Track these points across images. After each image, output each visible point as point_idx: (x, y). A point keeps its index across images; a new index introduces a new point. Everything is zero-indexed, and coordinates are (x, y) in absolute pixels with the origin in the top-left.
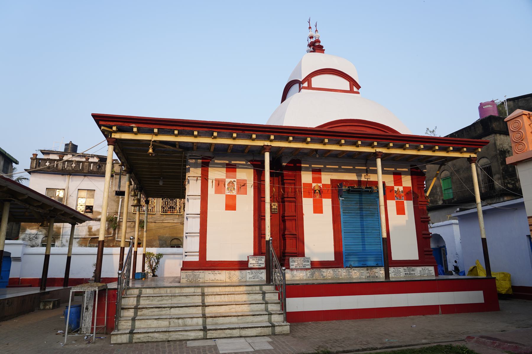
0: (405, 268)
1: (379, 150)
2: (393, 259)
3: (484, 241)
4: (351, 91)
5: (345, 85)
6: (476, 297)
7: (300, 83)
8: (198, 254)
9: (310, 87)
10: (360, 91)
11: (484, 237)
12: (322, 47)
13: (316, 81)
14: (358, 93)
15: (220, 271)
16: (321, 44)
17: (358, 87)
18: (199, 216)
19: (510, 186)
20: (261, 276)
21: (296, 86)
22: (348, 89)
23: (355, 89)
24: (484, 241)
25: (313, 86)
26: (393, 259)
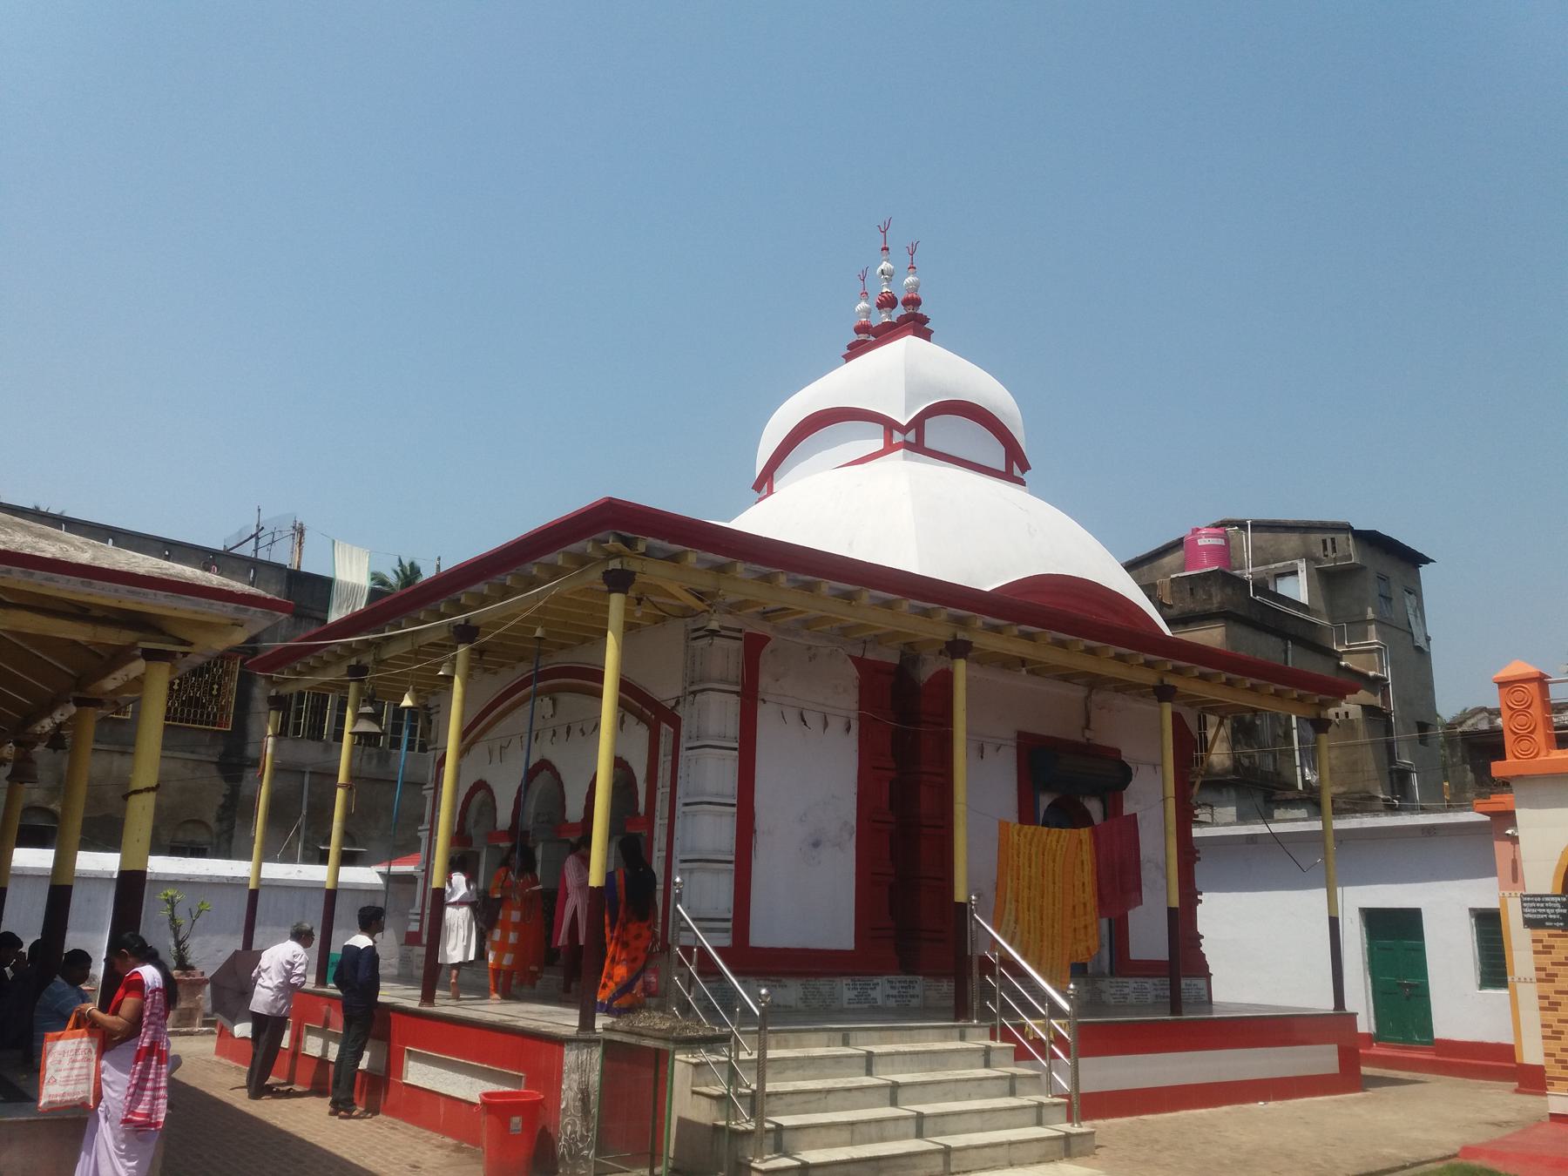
0: (1156, 980)
1: (1171, 680)
2: (1132, 957)
4: (1007, 476)
6: (1322, 1059)
7: (889, 425)
8: (729, 925)
9: (918, 447)
12: (926, 320)
13: (938, 433)
14: (1021, 482)
17: (1025, 467)
18: (734, 809)
19: (1246, 762)
20: (873, 994)
23: (1017, 471)
25: (929, 443)
26: (1132, 957)
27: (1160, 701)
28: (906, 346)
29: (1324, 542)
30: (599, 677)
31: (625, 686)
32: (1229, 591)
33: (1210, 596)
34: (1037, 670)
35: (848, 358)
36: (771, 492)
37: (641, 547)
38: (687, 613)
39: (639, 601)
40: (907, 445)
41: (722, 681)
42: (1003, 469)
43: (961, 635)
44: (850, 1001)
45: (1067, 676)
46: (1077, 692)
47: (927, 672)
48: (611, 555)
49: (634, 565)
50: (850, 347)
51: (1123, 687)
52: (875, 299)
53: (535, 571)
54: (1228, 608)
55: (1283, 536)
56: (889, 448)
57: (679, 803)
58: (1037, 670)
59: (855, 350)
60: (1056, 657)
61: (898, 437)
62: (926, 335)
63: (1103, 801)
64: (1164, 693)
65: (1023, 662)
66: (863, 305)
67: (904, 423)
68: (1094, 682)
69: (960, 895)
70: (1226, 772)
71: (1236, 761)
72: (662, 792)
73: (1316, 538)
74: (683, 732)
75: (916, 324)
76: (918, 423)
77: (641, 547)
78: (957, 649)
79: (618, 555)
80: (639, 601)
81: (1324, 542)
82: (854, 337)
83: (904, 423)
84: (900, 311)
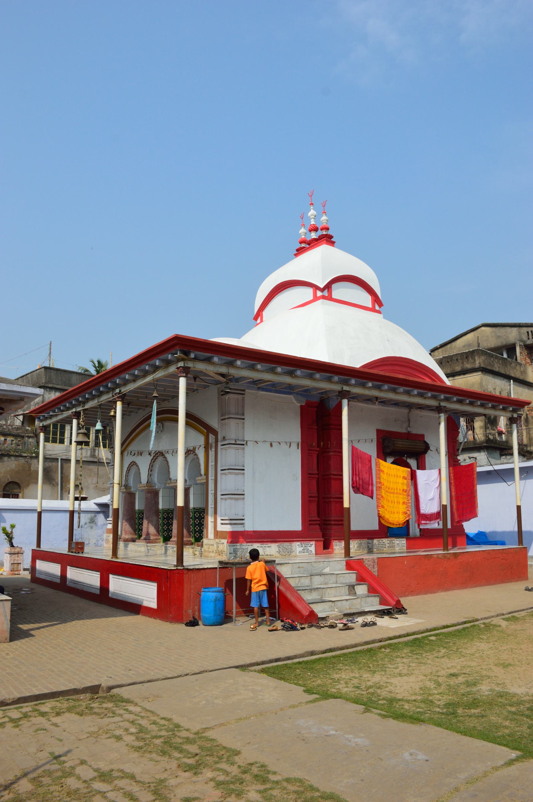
1: (443, 404)
3: (519, 508)
4: (373, 310)
5: (366, 300)
7: (315, 287)
9: (329, 298)
10: (382, 309)
11: (519, 504)
12: (331, 237)
13: (339, 291)
14: (379, 312)
15: (269, 545)
16: (330, 232)
19: (491, 437)
20: (310, 549)
21: (307, 293)
22: (370, 306)
23: (377, 308)
24: (519, 508)
25: (334, 296)
27: (439, 413)
28: (323, 249)
29: (528, 332)
30: (176, 412)
31: (188, 415)
32: (483, 358)
33: (475, 360)
34: (384, 402)
35: (296, 255)
36: (262, 321)
37: (192, 356)
38: (218, 383)
39: (195, 378)
40: (323, 297)
41: (236, 414)
42: (370, 306)
43: (346, 388)
44: (300, 552)
45: (397, 404)
46: (405, 411)
47: (332, 404)
48: (179, 360)
49: (190, 364)
50: (297, 250)
51: (421, 407)
52: (308, 227)
53: (147, 368)
54: (482, 366)
55: (509, 329)
56: (316, 298)
57: (219, 468)
58: (384, 402)
59: (300, 251)
60: (391, 396)
61: (319, 294)
62: (332, 243)
63: (417, 459)
64: (439, 410)
65: (377, 398)
66: (303, 230)
67: (322, 286)
68: (410, 406)
69: (346, 505)
70: (483, 442)
71: (486, 436)
72: (211, 463)
73: (525, 330)
74: (220, 437)
75: (328, 239)
76: (328, 286)
77: (192, 356)
78: (343, 394)
79: (183, 360)
80: (195, 378)
81: (528, 332)
82: (299, 246)
83: (322, 286)
84: (320, 233)
